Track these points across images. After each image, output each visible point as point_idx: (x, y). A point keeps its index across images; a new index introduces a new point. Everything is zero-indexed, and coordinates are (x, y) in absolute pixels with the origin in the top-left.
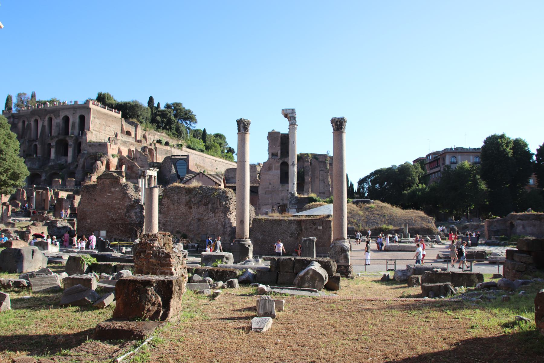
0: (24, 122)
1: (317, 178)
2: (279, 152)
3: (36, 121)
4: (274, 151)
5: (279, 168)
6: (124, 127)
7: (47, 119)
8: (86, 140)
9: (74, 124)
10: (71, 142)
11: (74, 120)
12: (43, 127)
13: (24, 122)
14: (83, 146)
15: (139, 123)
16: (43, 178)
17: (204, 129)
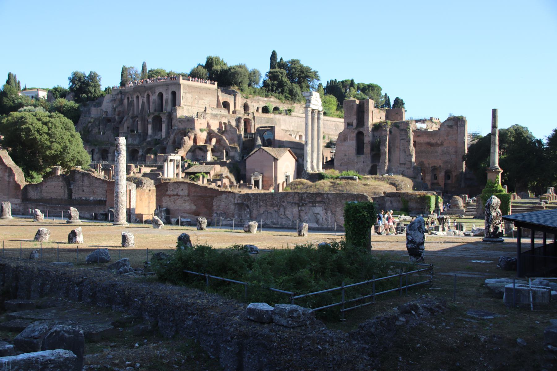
0: (128, 98)
1: (397, 147)
2: (355, 123)
3: (138, 97)
4: (350, 121)
5: (355, 139)
6: (220, 98)
7: (145, 96)
8: (177, 116)
9: (167, 100)
10: (164, 119)
11: (167, 96)
12: (143, 103)
13: (128, 98)
14: (174, 121)
15: (239, 91)
16: (140, 153)
17: (352, 80)
